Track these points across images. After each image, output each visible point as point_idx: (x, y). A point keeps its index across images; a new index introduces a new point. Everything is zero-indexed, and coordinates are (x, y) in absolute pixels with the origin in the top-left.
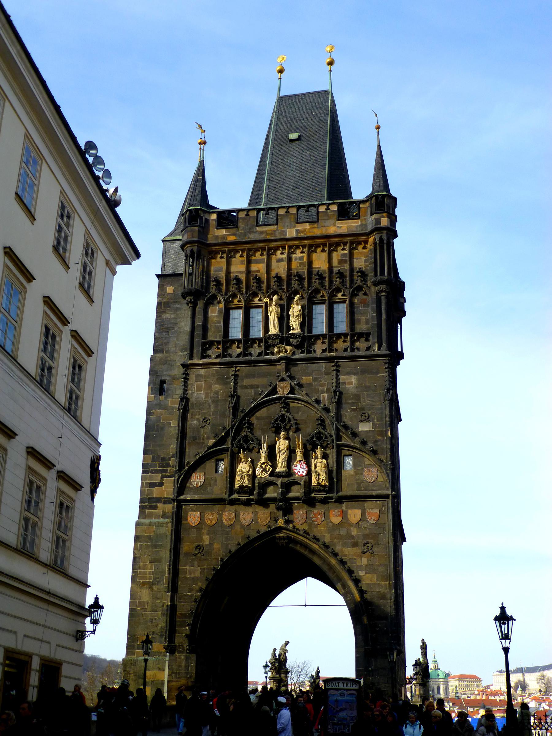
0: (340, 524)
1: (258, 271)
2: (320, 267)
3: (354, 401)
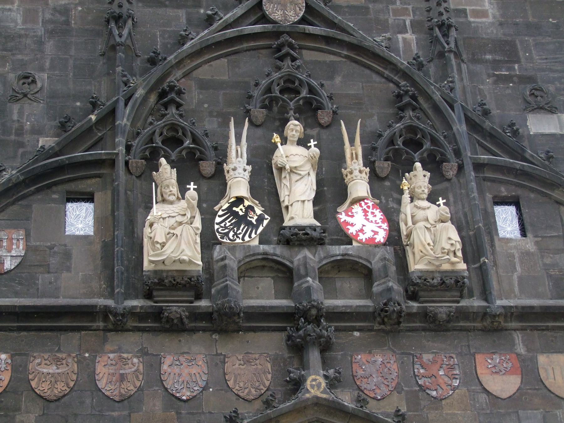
0: (516, 401)
3: (498, 58)
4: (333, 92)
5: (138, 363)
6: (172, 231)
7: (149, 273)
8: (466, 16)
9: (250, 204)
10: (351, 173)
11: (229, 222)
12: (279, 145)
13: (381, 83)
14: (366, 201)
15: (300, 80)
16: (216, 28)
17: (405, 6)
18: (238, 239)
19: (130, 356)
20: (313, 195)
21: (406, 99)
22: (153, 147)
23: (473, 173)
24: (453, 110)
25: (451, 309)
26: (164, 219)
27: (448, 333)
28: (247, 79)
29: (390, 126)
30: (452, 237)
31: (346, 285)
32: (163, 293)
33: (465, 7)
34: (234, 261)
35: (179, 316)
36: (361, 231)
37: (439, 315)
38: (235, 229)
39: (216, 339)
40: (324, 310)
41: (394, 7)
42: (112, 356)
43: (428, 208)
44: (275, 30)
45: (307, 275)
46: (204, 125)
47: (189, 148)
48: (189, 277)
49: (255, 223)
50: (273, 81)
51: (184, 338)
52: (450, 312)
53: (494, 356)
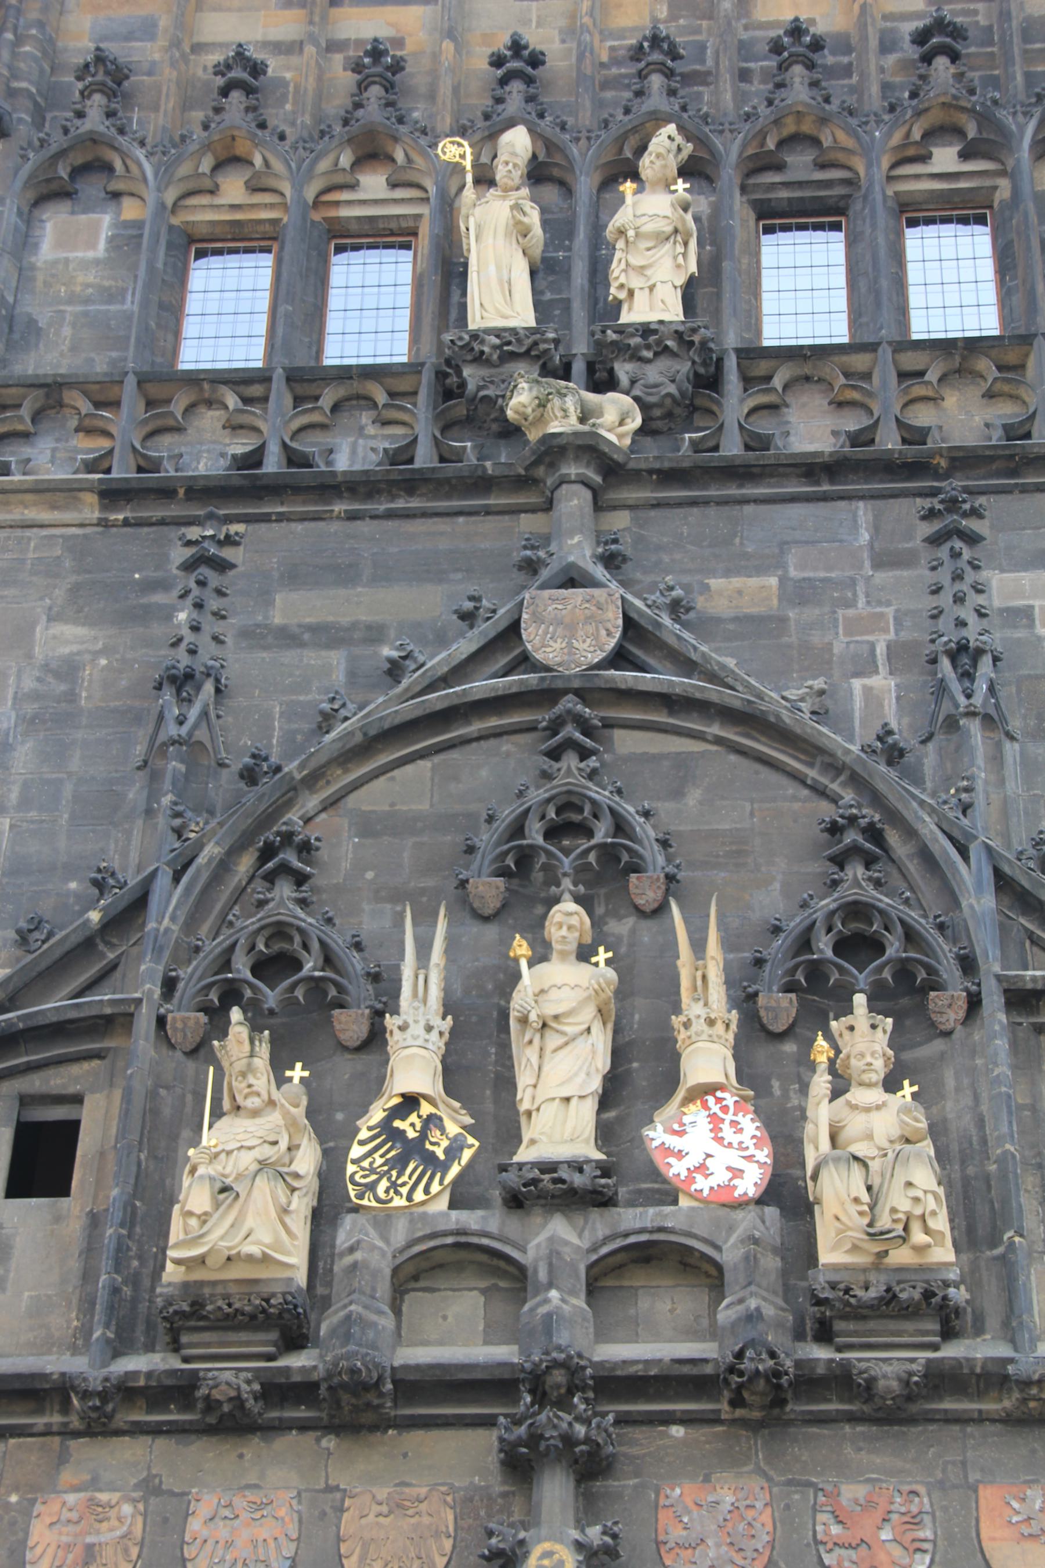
1: (399, 43)
2: (812, 21)
4: (672, 828)
5: (133, 1516)
6: (244, 1185)
7: (171, 1289)
8: (1031, 625)
9: (434, 1110)
10: (687, 1025)
11: (382, 1156)
12: (524, 964)
13: (795, 798)
14: (719, 1094)
15: (594, 802)
16: (407, 690)
17: (878, 610)
18: (397, 1199)
19: (114, 1497)
20: (596, 1084)
21: (851, 837)
22: (227, 980)
23: (1002, 1017)
24: (966, 858)
25: (914, 1367)
26: (229, 1153)
27: (913, 1429)
28: (473, 807)
29: (804, 905)
30: (915, 1182)
31: (663, 1306)
32: (206, 1336)
33: (1031, 602)
34: (383, 1254)
35: (233, 1394)
36: (702, 1168)
37: (882, 1383)
38: (394, 1173)
39: (328, 1449)
40: (589, 1371)
41: (851, 612)
42: (71, 1498)
43: (878, 1108)
44: (545, 685)
45: (550, 1285)
46: (361, 923)
47: (312, 978)
48: (265, 1296)
49: (442, 1157)
50: (528, 810)
51: (253, 1447)
52: (911, 1374)
53: (1029, 1492)
